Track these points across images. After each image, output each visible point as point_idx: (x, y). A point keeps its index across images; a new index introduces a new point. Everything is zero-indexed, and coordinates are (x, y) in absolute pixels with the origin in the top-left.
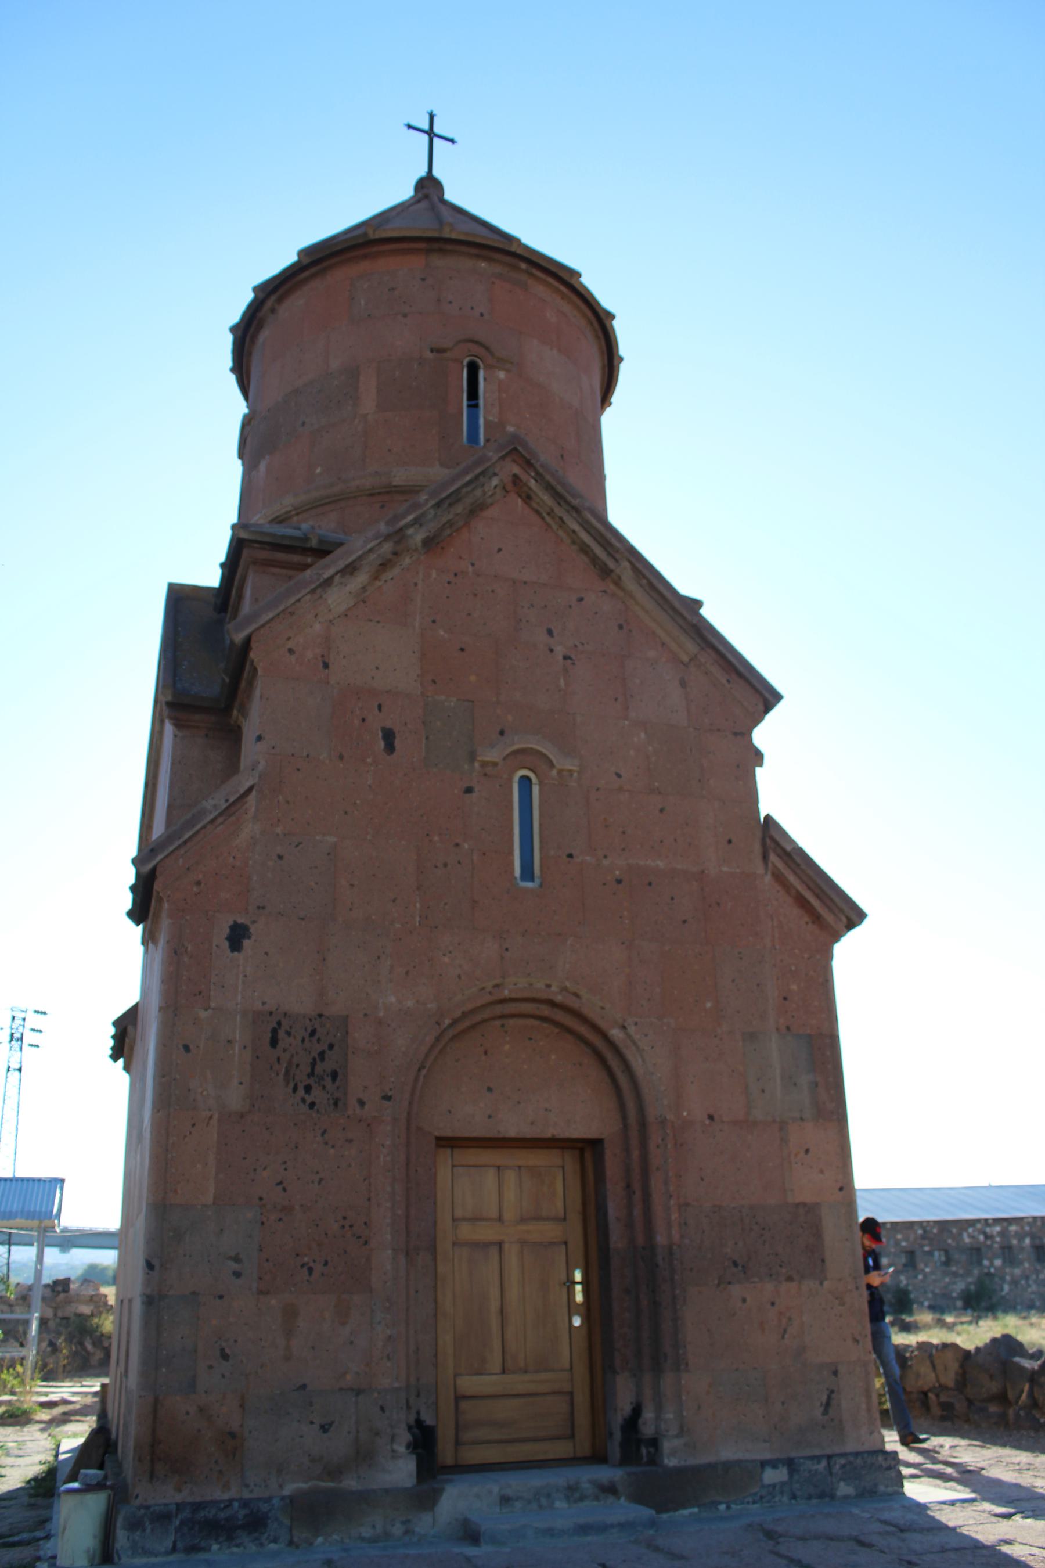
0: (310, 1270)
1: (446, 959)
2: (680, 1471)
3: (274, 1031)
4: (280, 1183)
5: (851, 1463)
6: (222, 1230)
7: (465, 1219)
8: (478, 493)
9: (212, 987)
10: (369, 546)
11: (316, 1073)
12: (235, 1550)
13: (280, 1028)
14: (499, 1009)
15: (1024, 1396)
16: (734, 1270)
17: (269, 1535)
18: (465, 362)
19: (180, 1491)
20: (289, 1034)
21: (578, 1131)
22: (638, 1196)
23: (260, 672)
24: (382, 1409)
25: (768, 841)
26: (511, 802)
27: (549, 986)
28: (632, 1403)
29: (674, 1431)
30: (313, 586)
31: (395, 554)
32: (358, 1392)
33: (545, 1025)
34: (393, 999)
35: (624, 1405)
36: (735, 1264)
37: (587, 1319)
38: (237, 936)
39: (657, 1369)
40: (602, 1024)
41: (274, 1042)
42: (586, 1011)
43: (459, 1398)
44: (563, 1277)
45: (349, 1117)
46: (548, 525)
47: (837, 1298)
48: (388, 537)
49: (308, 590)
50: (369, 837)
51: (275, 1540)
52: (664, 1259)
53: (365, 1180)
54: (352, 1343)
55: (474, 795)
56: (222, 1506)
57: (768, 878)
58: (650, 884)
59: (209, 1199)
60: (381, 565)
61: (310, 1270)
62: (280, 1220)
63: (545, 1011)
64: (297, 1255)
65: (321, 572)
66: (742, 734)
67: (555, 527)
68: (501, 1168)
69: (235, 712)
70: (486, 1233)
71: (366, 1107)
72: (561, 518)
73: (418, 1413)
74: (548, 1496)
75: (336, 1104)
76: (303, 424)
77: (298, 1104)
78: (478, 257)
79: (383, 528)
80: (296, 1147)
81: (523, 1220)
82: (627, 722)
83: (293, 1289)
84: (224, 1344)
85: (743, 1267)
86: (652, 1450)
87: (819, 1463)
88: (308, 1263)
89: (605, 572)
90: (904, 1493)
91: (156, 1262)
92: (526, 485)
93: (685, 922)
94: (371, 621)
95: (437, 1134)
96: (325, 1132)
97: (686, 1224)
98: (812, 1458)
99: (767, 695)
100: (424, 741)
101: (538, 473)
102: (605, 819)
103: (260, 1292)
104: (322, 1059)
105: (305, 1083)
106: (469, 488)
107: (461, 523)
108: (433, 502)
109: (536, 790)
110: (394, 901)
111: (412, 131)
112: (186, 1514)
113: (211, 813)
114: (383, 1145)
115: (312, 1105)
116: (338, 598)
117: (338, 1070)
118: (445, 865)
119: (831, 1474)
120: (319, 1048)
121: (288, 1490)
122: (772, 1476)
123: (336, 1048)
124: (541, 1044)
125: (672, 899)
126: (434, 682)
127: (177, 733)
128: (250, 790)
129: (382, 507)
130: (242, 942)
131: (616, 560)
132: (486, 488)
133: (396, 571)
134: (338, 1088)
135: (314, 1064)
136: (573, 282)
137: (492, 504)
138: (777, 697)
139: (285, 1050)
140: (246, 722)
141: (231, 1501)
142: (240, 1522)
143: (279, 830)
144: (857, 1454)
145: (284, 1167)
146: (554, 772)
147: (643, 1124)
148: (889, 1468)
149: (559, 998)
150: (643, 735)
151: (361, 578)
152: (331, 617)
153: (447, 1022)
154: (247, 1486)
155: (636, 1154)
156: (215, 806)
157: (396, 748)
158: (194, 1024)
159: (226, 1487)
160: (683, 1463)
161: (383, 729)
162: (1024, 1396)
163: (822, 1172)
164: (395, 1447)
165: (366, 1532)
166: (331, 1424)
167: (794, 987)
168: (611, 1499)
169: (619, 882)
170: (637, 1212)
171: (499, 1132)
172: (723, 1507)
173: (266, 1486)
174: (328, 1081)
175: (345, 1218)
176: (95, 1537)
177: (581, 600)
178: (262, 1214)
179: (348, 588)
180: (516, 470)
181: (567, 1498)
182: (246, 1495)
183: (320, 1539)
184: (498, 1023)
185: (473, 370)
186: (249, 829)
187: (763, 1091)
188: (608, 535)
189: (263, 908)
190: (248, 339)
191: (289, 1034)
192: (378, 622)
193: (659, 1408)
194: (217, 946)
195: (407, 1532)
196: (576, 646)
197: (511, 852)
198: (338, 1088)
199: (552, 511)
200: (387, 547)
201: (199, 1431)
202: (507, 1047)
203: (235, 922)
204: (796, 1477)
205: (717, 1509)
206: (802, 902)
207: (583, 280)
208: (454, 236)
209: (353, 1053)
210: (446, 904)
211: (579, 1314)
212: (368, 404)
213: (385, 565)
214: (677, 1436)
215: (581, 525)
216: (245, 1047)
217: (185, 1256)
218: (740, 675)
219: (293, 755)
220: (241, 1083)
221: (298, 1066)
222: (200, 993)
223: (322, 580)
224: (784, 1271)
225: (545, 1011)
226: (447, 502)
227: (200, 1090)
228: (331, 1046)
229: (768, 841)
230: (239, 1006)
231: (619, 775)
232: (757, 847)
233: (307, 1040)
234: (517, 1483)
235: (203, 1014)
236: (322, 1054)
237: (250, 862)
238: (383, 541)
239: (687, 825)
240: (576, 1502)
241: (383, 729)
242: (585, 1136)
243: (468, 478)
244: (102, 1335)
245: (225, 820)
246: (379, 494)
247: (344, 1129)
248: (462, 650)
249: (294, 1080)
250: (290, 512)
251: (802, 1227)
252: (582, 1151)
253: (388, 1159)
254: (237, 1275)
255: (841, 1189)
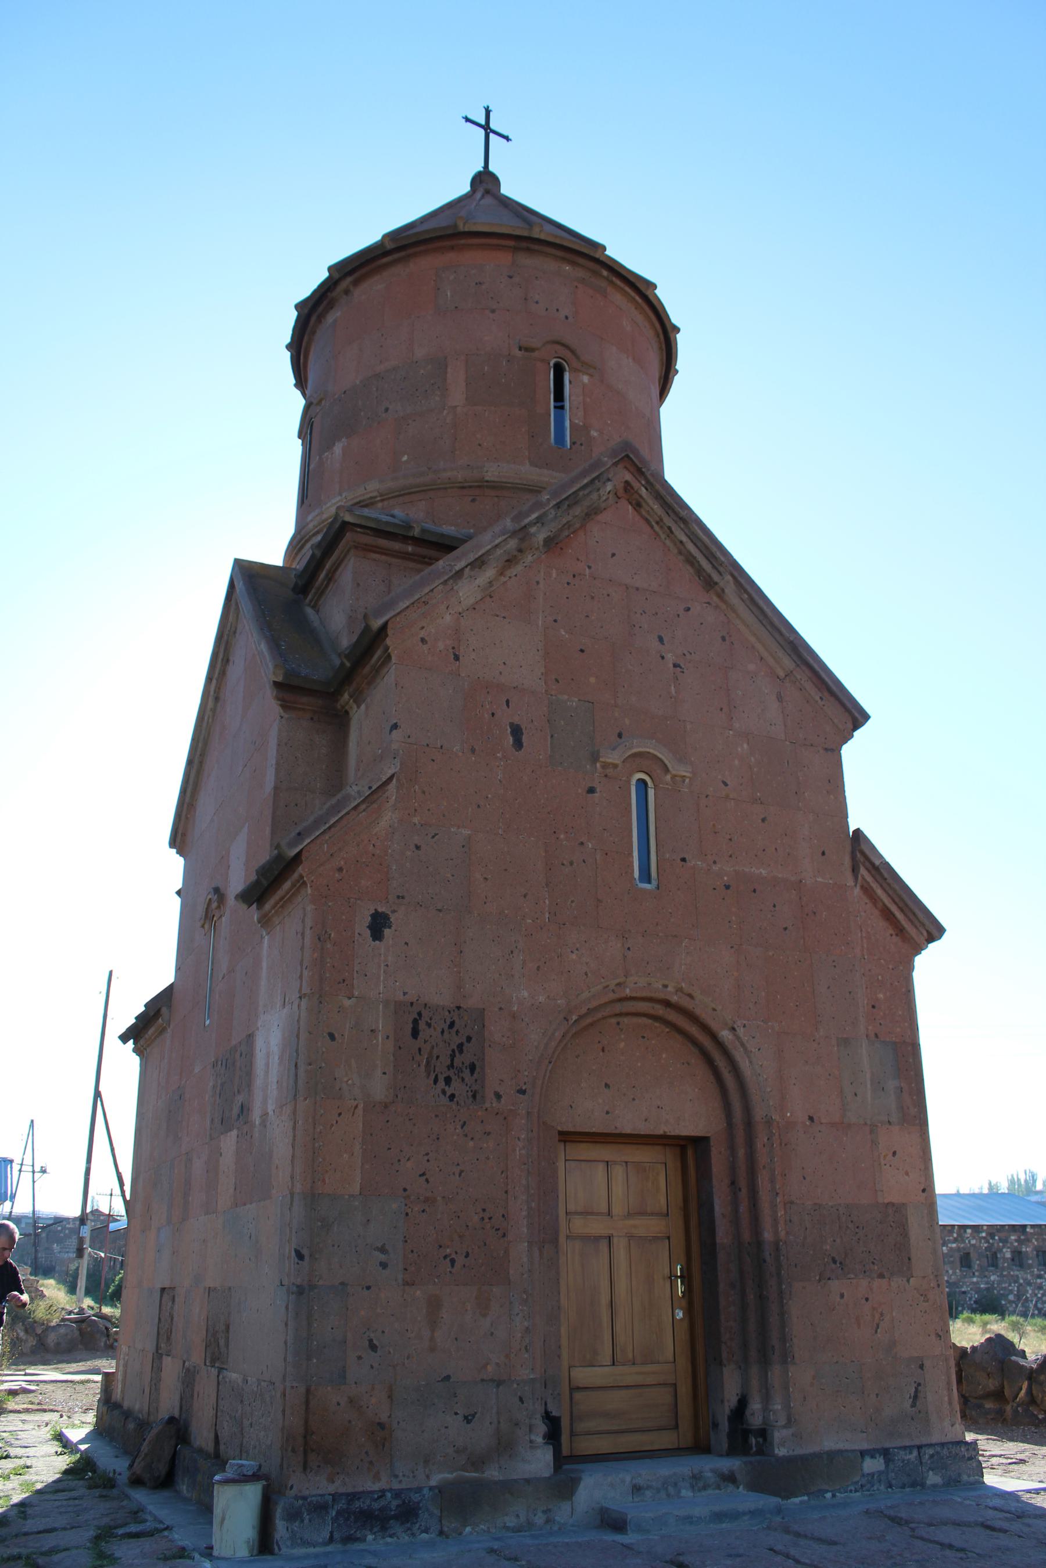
0: (453, 1261)
1: (574, 956)
2: (790, 1460)
3: (415, 1022)
4: (423, 1174)
5: (938, 1453)
6: (368, 1220)
7: (576, 1213)
8: (594, 496)
9: (355, 974)
10: (497, 542)
11: (455, 1064)
12: (389, 1540)
13: (420, 1019)
14: (619, 1008)
15: (1023, 1392)
16: (833, 1266)
17: (421, 1525)
18: (552, 364)
19: (333, 1482)
20: (429, 1025)
21: (687, 1129)
22: (744, 1193)
23: (394, 659)
24: (521, 1400)
25: (859, 855)
26: (630, 804)
27: (665, 986)
28: (737, 1394)
29: (782, 1421)
30: (446, 578)
31: (520, 551)
32: (499, 1383)
33: (657, 1024)
34: (526, 994)
35: (731, 1396)
36: (834, 1261)
37: (689, 1311)
38: (378, 925)
39: (765, 1361)
40: (714, 1025)
41: (415, 1033)
42: (698, 1011)
43: (574, 1389)
44: (667, 1271)
45: (486, 1110)
46: (657, 534)
47: (922, 1295)
48: (514, 534)
49: (442, 580)
50: (500, 832)
51: (426, 1531)
52: (770, 1255)
53: (502, 1172)
54: (492, 1334)
55: (596, 795)
56: (376, 1496)
57: (857, 891)
58: (755, 891)
59: (356, 1189)
60: (508, 561)
61: (453, 1261)
62: (423, 1211)
63: (660, 1010)
64: (441, 1247)
65: (453, 564)
66: (832, 750)
67: (663, 536)
68: (609, 1163)
69: (346, 696)
70: (597, 1227)
71: (503, 1101)
72: (669, 528)
73: (546, 1404)
74: (676, 1484)
75: (474, 1096)
76: (387, 410)
77: (439, 1096)
78: (563, 259)
79: (508, 523)
80: (438, 1139)
81: (629, 1215)
82: (731, 732)
83: (436, 1280)
84: (372, 1335)
85: (841, 1263)
86: (760, 1440)
87: (911, 1453)
88: (450, 1254)
89: (709, 584)
90: (984, 1483)
91: (305, 1252)
92: (636, 492)
93: (785, 929)
94: (498, 616)
95: (559, 1129)
96: (465, 1123)
97: (790, 1221)
98: (905, 1448)
99: (857, 715)
100: (549, 737)
101: (648, 481)
102: (714, 825)
103: (406, 1283)
104: (461, 1051)
105: (445, 1075)
106: (586, 492)
107: (578, 525)
108: (555, 503)
109: (651, 793)
110: (525, 896)
111: (469, 124)
112: (342, 1505)
113: (355, 799)
114: (519, 1139)
115: (452, 1097)
116: (468, 591)
117: (476, 1062)
118: (571, 863)
119: (921, 1463)
120: (457, 1040)
121: (433, 1482)
122: (872, 1465)
123: (474, 1040)
124: (653, 1042)
125: (774, 906)
126: (557, 681)
127: (283, 714)
128: (392, 776)
129: (473, 500)
130: (383, 931)
131: (720, 574)
132: (601, 492)
133: (518, 569)
134: (476, 1080)
135: (453, 1056)
136: (648, 293)
137: (605, 509)
138: (866, 717)
139: (425, 1042)
140: (358, 707)
141: (382, 1493)
142: (393, 1513)
143: (416, 820)
144: (943, 1445)
145: (426, 1158)
146: (668, 777)
147: (749, 1124)
148: (970, 1458)
149: (674, 999)
150: (745, 746)
151: (490, 573)
152: (460, 610)
153: (574, 1018)
154: (396, 1476)
155: (741, 1153)
156: (359, 792)
157: (524, 744)
158: (339, 1012)
159: (377, 1477)
160: (791, 1453)
161: (512, 725)
162: (1023, 1392)
163: (907, 1174)
164: (533, 1437)
165: (511, 1521)
166: (474, 1416)
167: (881, 996)
168: (731, 1487)
169: (727, 887)
170: (743, 1208)
171: (616, 1128)
172: (829, 1495)
173: (414, 1477)
174: (466, 1073)
175: (484, 1210)
176: (254, 1527)
177: (688, 609)
178: (406, 1205)
179: (477, 582)
180: (628, 477)
181: (692, 1487)
182: (396, 1486)
183: (468, 1529)
184: (614, 1021)
185: (559, 371)
186: (388, 818)
187: (856, 1095)
188: (714, 549)
189: (403, 897)
190: (313, 319)
191: (429, 1025)
192: (504, 618)
193: (767, 1399)
194: (359, 934)
195: (547, 1521)
196: (684, 655)
197: (631, 854)
198: (476, 1080)
199: (661, 520)
200: (513, 544)
201: (350, 1422)
202: (622, 1045)
203: (376, 910)
204: (891, 1466)
205: (825, 1497)
206: (887, 915)
207: (658, 292)
208: (542, 237)
209: (490, 1046)
210: (572, 902)
211: (681, 1309)
212: (457, 395)
213: (511, 561)
214: (785, 1427)
215: (689, 537)
216: (388, 1037)
217: (333, 1246)
218: (832, 693)
219: (428, 745)
220: (384, 1073)
221: (438, 1057)
222: (344, 980)
223: (454, 572)
224: (876, 1268)
225: (660, 1010)
226: (567, 503)
227: (345, 1079)
228: (469, 1039)
229: (859, 855)
230: (381, 995)
231: (726, 784)
232: (847, 862)
233: (446, 1033)
234: (646, 1472)
235: (347, 1003)
236: (460, 1046)
237: (390, 851)
238: (509, 537)
239: (786, 835)
240: (699, 1491)
241: (512, 725)
242: (693, 1134)
243: (585, 481)
244: (35, 1322)
245: (368, 807)
246: (470, 487)
247: (482, 1122)
248: (582, 651)
249: (434, 1071)
250: (376, 497)
251: (891, 1226)
252: (683, 1149)
253: (523, 1152)
254: (384, 1265)
255: (924, 1191)
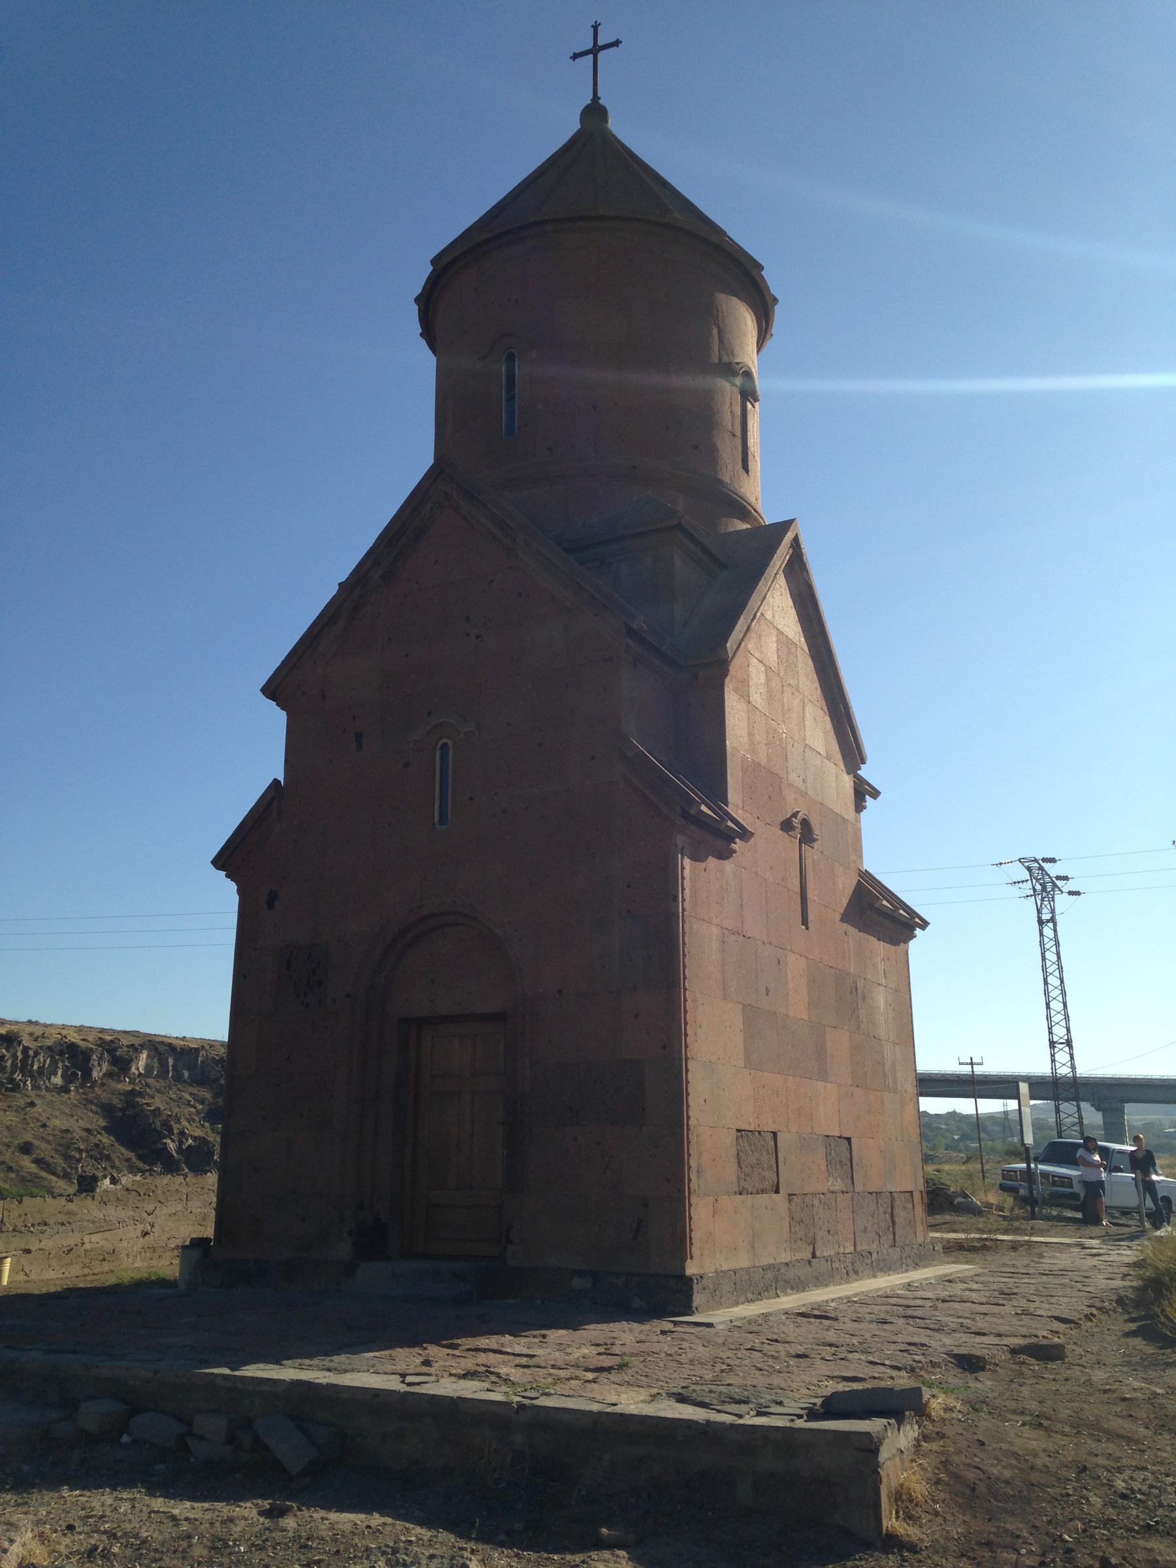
128: (273, 798)
187: (604, 967)
